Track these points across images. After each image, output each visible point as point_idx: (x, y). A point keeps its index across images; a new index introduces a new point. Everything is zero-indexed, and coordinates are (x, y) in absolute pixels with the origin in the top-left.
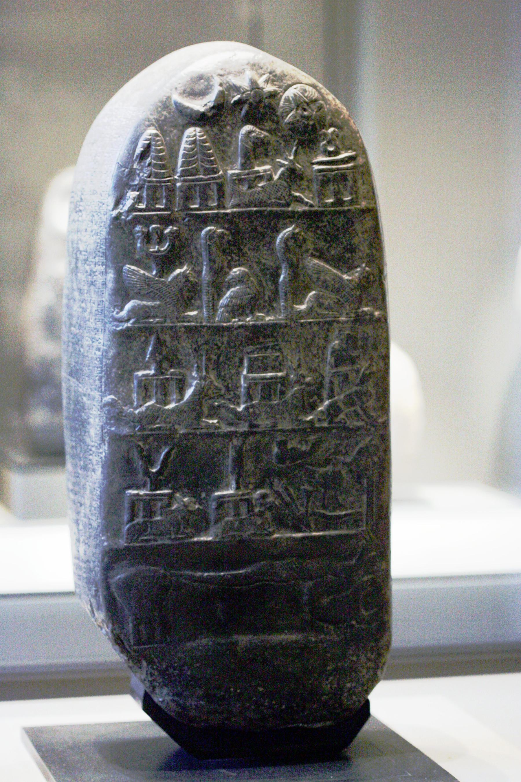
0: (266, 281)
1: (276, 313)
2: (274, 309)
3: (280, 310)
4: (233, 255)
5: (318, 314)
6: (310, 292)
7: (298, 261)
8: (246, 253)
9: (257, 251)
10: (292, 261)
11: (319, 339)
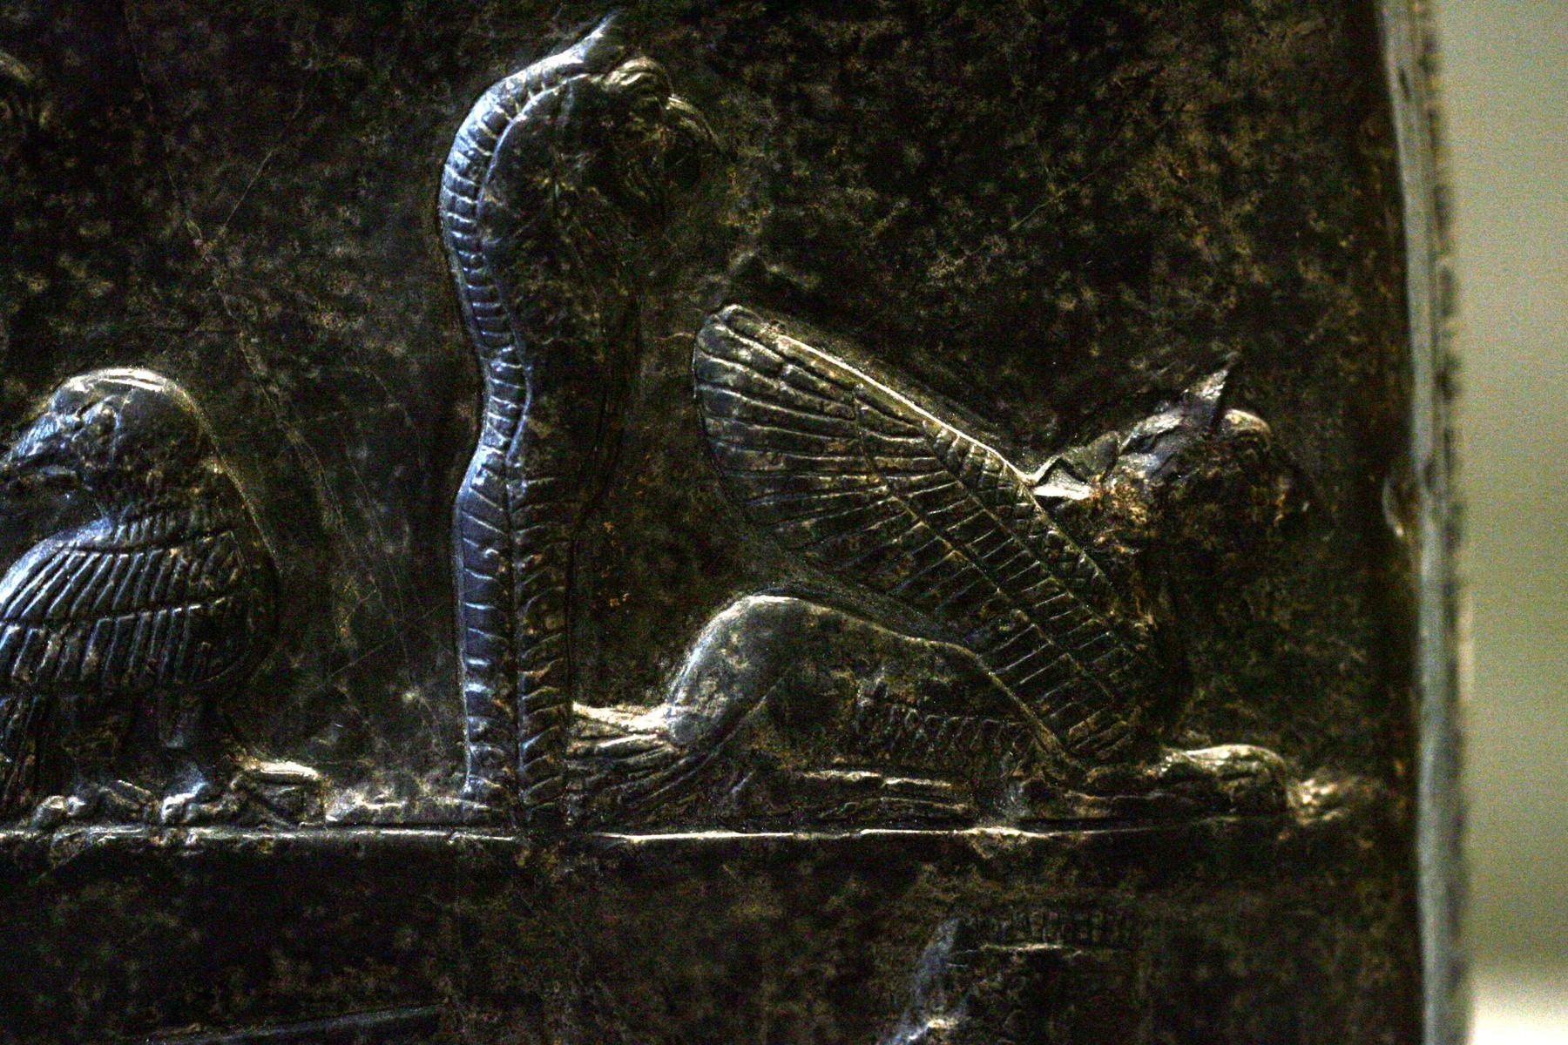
0: (344, 487)
1: (423, 767)
2: (400, 723)
3: (453, 734)
4: (64, 260)
5: (782, 790)
6: (721, 600)
7: (625, 324)
8: (186, 251)
9: (278, 233)
10: (568, 328)
11: (791, 990)
